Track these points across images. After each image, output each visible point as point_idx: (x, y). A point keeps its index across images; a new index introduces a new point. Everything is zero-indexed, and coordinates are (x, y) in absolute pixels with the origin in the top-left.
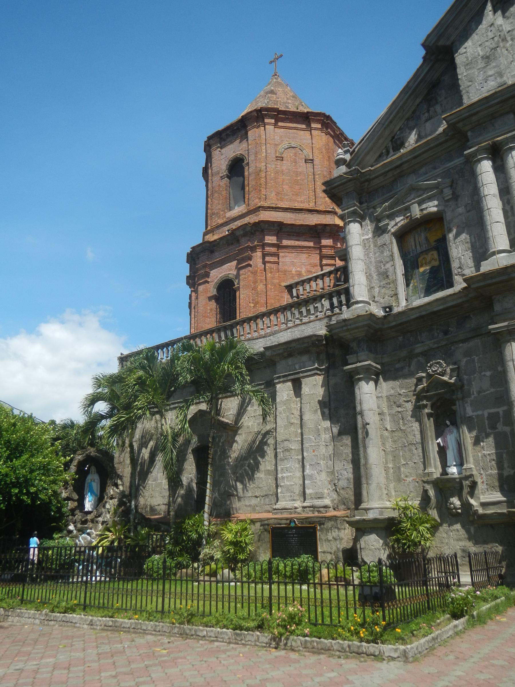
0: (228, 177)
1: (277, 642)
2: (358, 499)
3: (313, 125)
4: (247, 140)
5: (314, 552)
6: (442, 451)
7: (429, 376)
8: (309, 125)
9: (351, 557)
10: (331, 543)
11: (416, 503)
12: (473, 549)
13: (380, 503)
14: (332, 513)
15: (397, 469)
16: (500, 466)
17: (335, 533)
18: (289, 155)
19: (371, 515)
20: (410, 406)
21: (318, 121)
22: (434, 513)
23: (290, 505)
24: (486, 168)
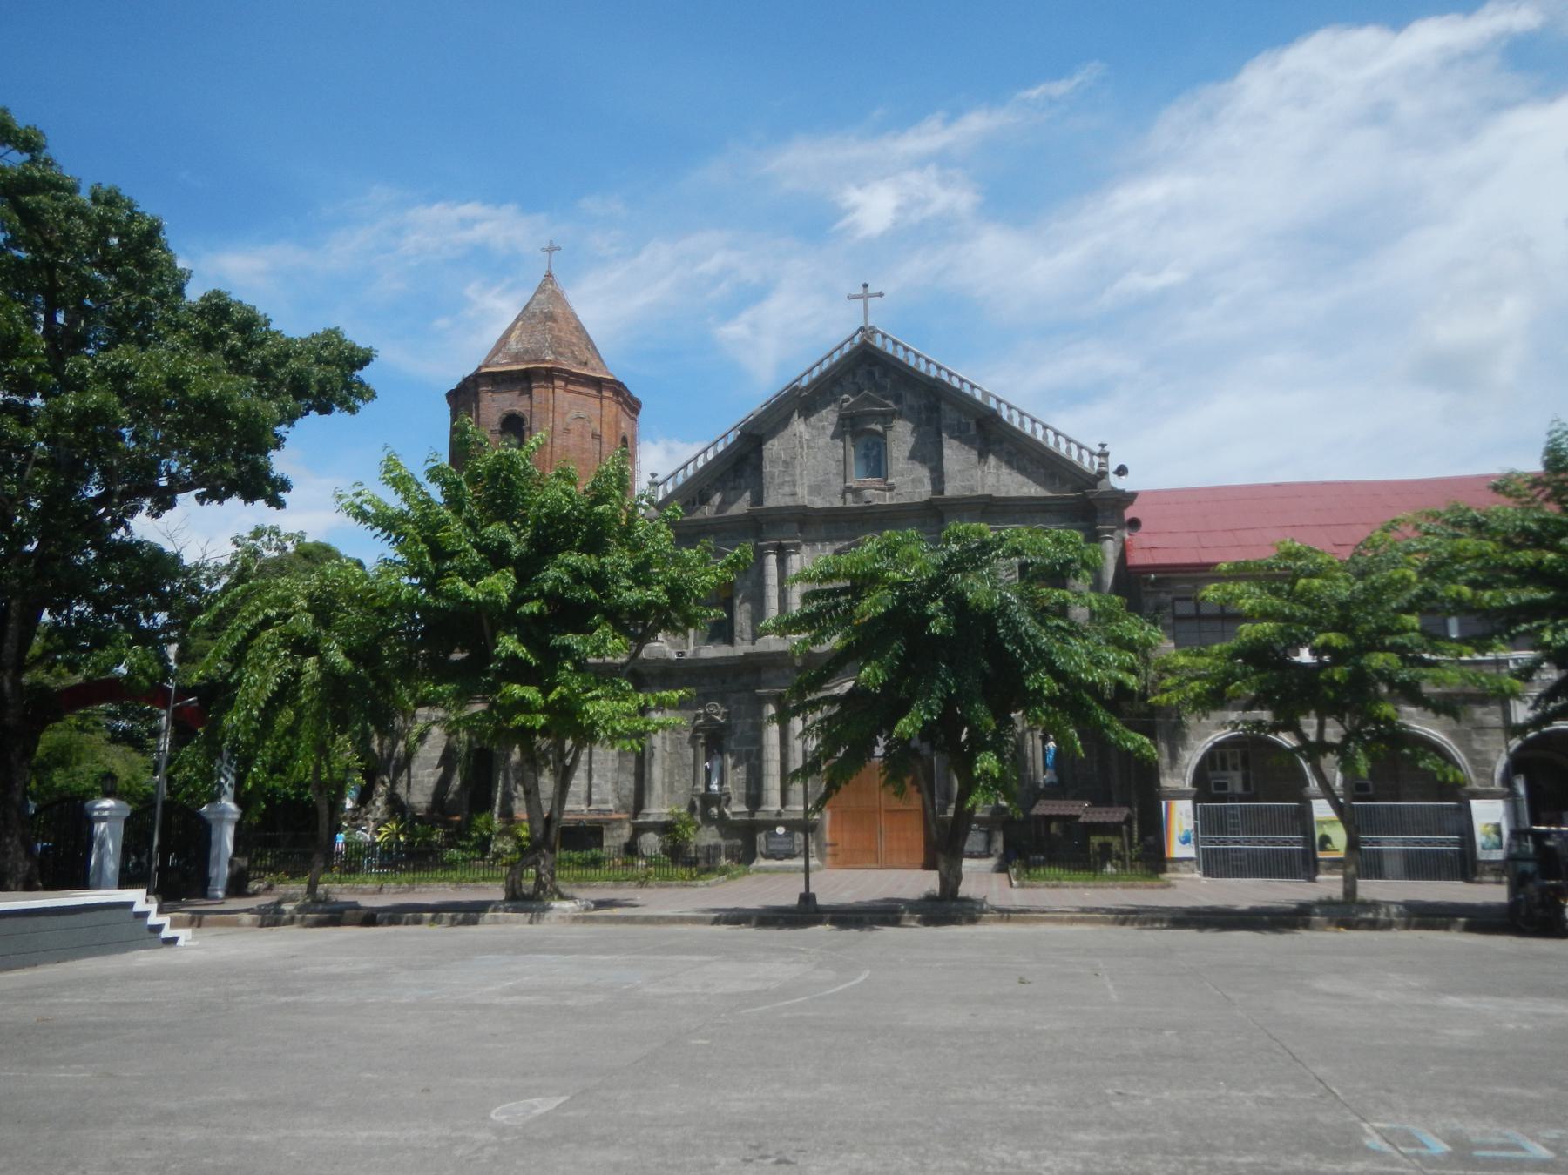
0: (501, 433)
1: (641, 884)
2: (639, 804)
3: (606, 394)
4: (531, 398)
5: (600, 845)
6: (708, 772)
7: (706, 714)
8: (600, 391)
9: (631, 849)
10: (615, 839)
11: (683, 810)
12: (723, 843)
13: (659, 808)
14: (615, 816)
15: (671, 784)
16: (748, 788)
17: (619, 832)
18: (576, 427)
19: (650, 819)
20: (687, 735)
21: (610, 389)
22: (698, 818)
23: (576, 807)
24: (772, 560)
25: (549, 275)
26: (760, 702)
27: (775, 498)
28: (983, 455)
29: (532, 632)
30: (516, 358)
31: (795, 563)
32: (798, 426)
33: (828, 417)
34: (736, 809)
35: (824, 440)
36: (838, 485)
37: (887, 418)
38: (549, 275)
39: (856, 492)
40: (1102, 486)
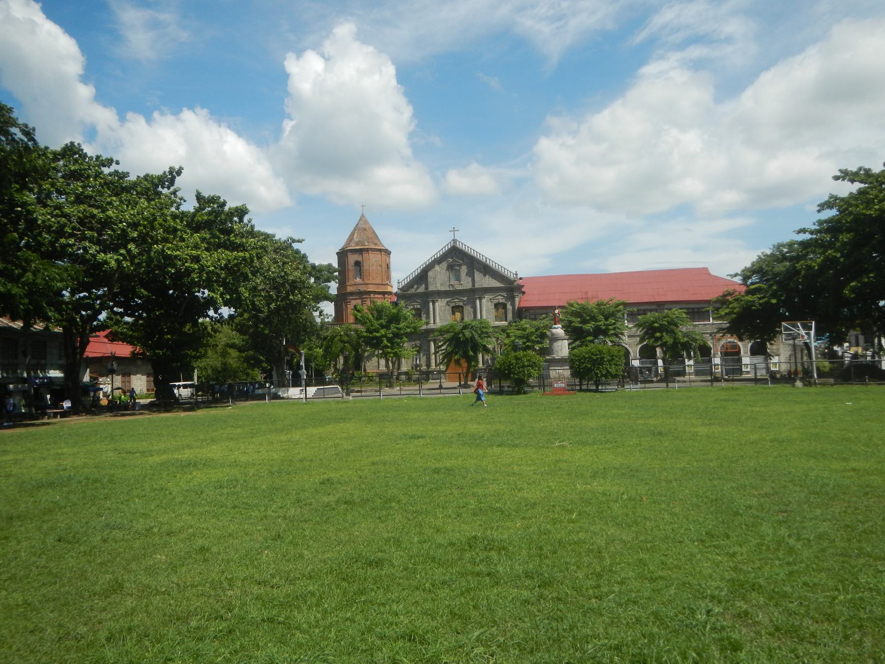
9: (397, 378)
13: (404, 368)
25: (363, 215)
26: (429, 341)
27: (431, 288)
28: (485, 275)
29: (389, 340)
30: (357, 244)
31: (437, 304)
32: (437, 268)
33: (444, 265)
34: (424, 368)
35: (444, 271)
36: (448, 283)
37: (460, 266)
38: (363, 215)
39: (453, 286)
40: (515, 284)
